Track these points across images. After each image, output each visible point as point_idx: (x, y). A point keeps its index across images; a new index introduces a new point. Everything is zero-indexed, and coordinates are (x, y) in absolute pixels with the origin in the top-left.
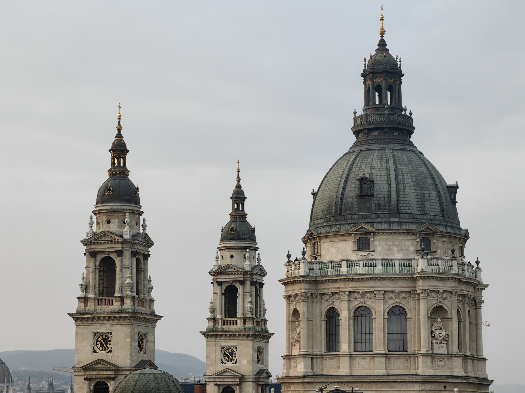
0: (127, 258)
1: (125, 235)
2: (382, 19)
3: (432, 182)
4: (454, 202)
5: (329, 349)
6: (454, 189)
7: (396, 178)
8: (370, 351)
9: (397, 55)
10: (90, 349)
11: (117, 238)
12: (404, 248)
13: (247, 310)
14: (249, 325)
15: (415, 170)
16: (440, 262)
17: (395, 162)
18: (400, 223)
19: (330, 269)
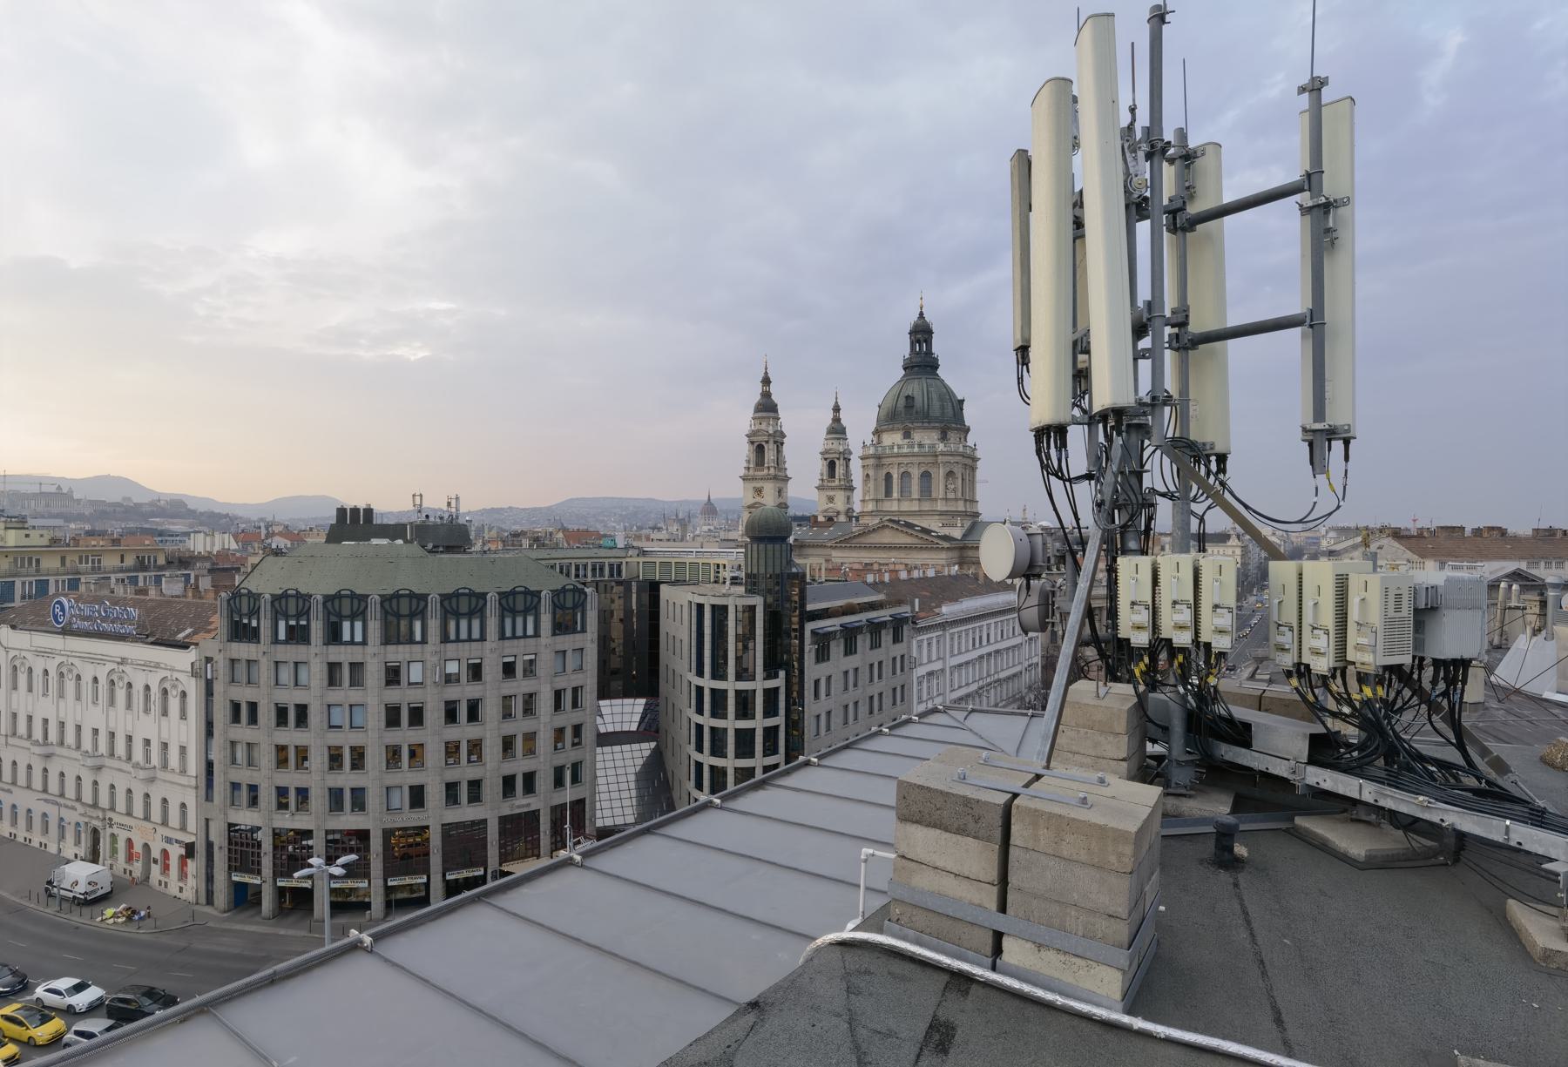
4: (962, 409)
5: (886, 497)
6: (962, 402)
13: (841, 474)
14: (842, 483)
16: (952, 445)
18: (929, 422)
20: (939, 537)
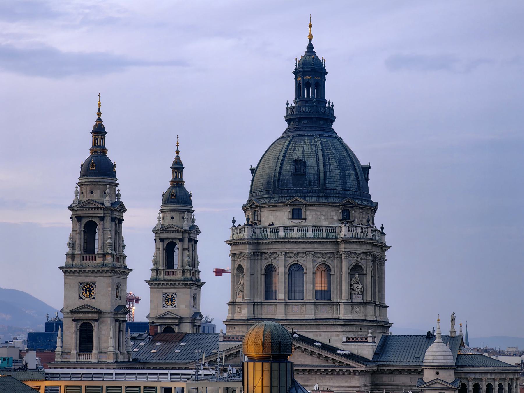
0: (108, 222)
1: (106, 203)
2: (310, 26)
3: (351, 163)
4: (367, 180)
5: (266, 299)
6: (366, 169)
7: (324, 160)
8: (301, 300)
9: (323, 57)
10: (77, 296)
11: (100, 206)
12: (329, 217)
14: (187, 275)
15: (338, 153)
17: (322, 147)
18: (327, 197)
19: (269, 234)
20: (345, 356)
